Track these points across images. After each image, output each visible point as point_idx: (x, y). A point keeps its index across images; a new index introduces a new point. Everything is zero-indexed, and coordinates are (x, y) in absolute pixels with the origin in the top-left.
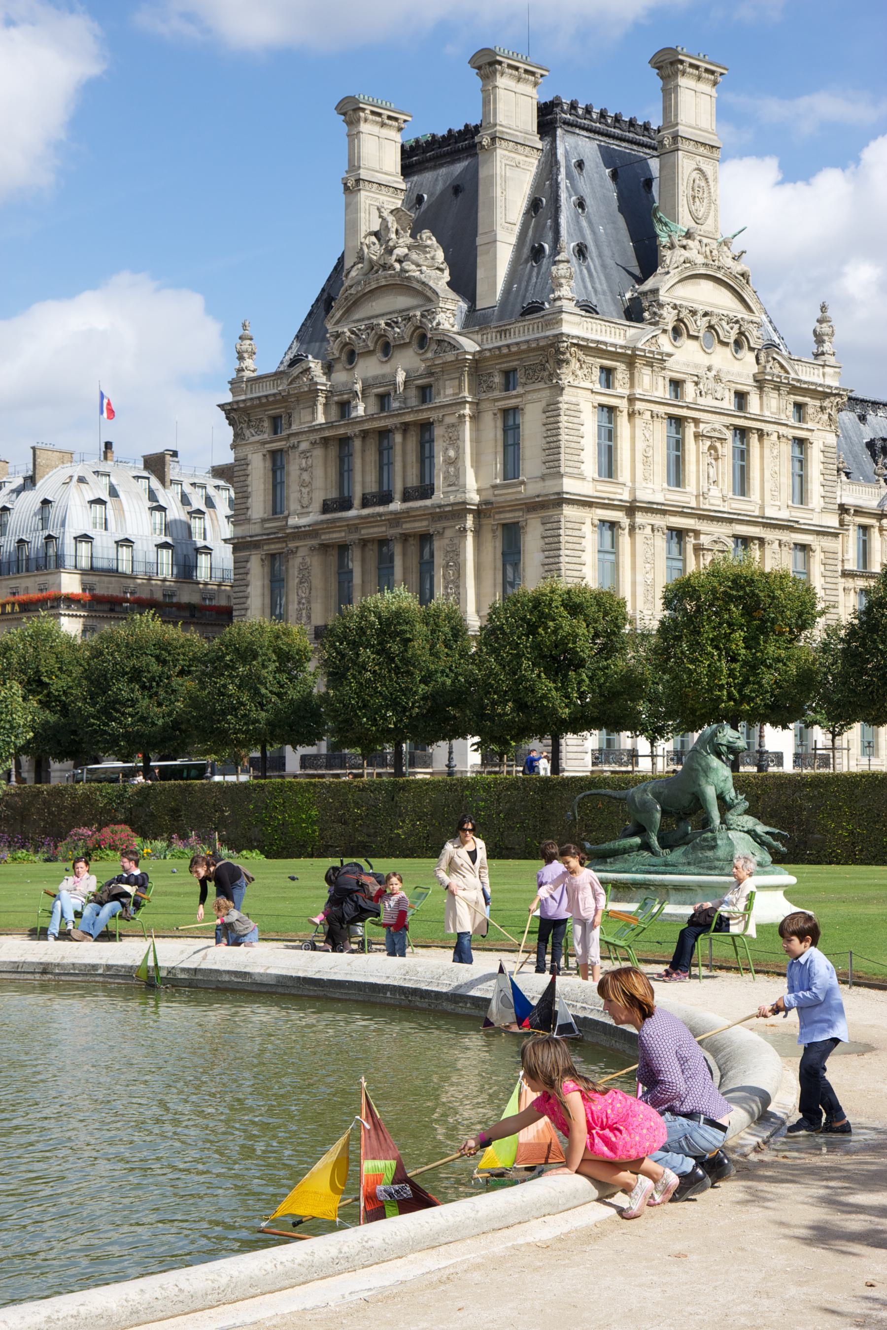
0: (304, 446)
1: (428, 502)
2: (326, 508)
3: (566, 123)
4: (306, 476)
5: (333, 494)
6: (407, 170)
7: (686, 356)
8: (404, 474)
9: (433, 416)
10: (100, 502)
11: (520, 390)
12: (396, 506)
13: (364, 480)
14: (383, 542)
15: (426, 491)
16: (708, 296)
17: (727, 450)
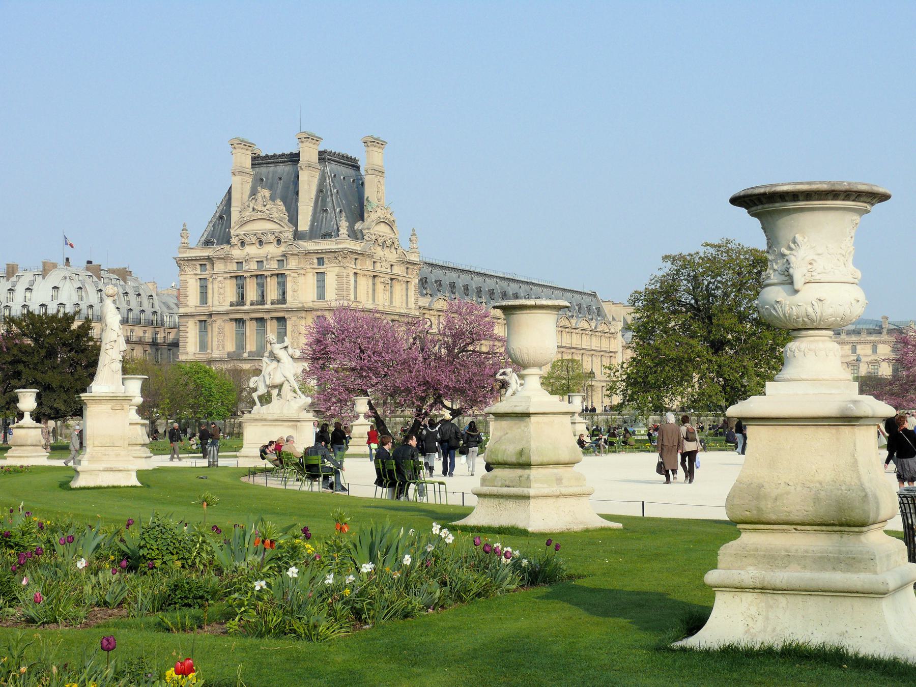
0: (219, 279)
1: (284, 306)
2: (232, 305)
3: (329, 160)
4: (221, 291)
5: (234, 299)
6: (253, 165)
7: (379, 252)
8: (272, 293)
9: (287, 273)
10: (80, 288)
11: (325, 266)
12: (268, 306)
13: (252, 294)
14: (261, 320)
15: (283, 300)
16: (383, 229)
17: (388, 287)
